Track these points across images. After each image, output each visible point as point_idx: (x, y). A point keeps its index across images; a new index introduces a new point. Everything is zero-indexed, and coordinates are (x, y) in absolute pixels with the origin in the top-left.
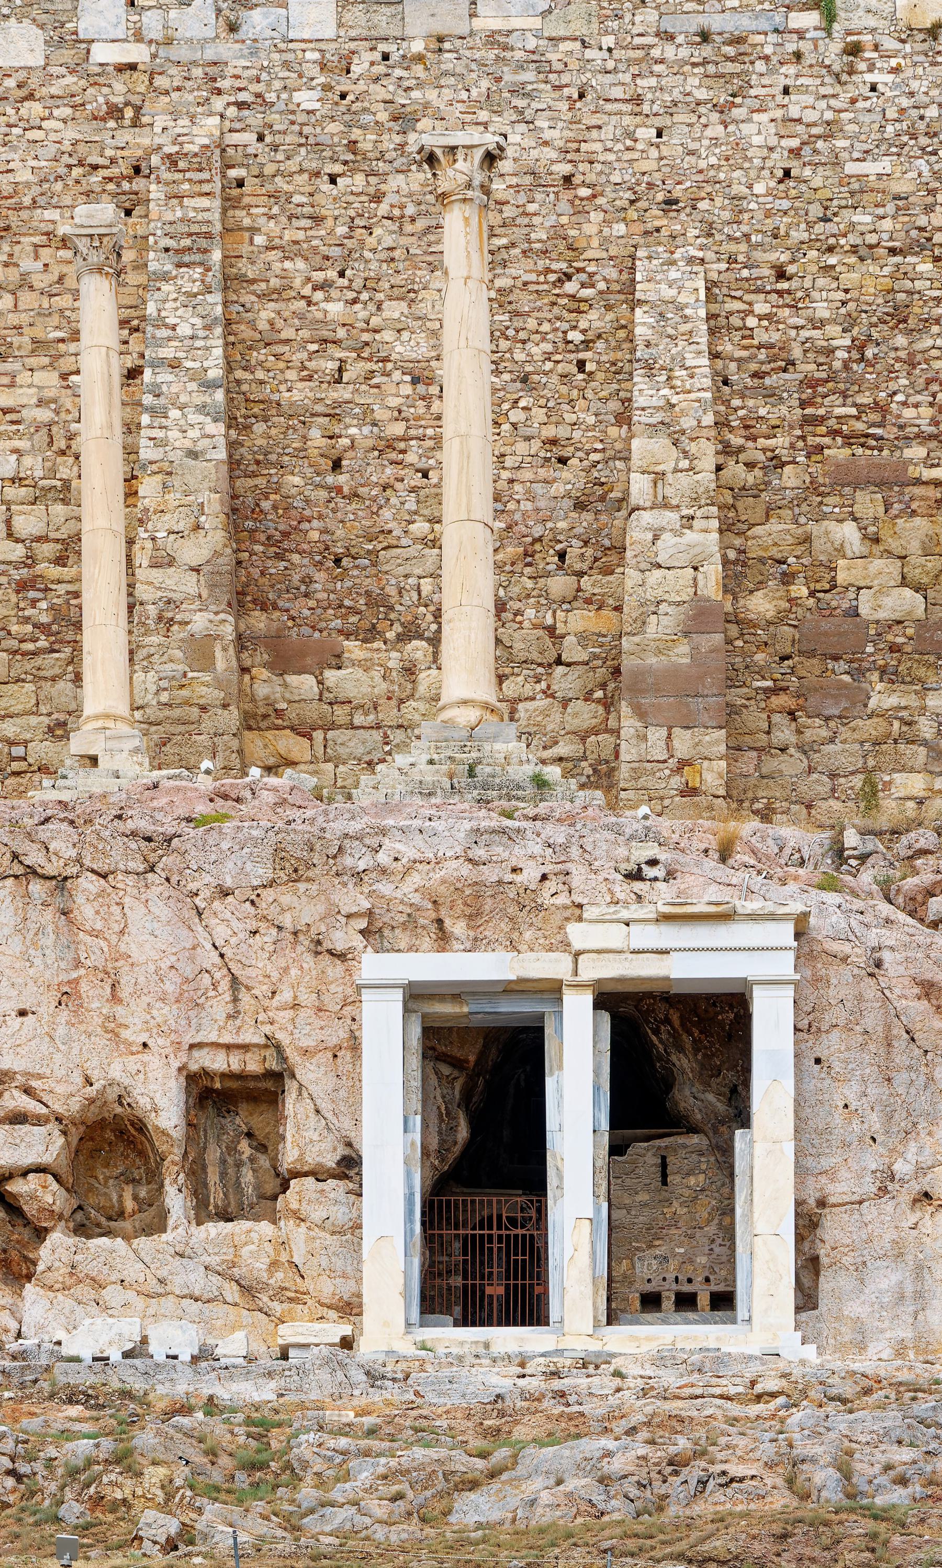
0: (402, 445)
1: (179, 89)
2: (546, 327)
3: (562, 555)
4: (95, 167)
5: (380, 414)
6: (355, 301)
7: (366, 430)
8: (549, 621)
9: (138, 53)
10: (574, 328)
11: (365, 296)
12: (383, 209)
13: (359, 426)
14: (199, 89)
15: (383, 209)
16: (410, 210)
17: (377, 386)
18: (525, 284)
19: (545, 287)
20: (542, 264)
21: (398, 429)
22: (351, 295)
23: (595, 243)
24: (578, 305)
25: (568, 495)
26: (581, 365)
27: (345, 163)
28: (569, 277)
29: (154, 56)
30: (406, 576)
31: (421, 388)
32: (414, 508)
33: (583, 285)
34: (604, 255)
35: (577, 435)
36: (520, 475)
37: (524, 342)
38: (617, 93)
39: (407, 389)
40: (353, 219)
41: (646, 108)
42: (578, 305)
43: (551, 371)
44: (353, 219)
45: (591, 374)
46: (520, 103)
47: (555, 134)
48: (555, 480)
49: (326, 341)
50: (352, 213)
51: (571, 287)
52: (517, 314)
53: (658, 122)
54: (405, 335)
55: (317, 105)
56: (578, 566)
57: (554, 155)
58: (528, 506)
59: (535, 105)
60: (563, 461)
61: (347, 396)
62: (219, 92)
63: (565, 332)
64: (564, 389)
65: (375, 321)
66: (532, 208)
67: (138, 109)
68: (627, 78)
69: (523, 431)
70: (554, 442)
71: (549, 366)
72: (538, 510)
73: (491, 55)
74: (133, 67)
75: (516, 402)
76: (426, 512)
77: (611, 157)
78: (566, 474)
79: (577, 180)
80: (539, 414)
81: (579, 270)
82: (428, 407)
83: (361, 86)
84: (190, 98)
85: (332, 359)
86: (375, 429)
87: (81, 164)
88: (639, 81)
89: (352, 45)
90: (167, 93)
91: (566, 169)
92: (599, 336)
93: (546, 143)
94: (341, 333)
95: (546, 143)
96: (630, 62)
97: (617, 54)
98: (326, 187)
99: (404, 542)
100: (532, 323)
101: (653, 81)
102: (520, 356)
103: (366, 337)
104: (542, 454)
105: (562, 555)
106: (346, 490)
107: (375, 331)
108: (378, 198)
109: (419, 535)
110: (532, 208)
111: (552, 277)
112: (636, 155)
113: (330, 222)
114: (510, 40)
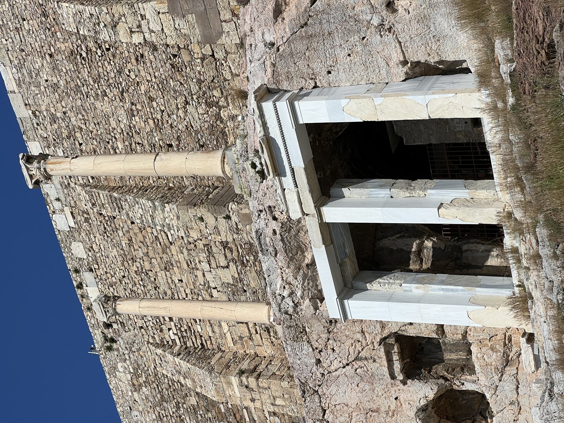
0: (156, 120)
1: (73, 198)
2: (100, 64)
3: (175, 56)
4: (105, 228)
5: (148, 129)
6: (115, 138)
7: (155, 135)
8: (199, 61)
9: (67, 210)
10: (97, 53)
11: (112, 134)
12: (83, 127)
13: (155, 137)
14: (70, 191)
15: (83, 127)
16: (80, 116)
17: (140, 130)
18: (89, 73)
19: (87, 64)
20: (81, 66)
21: (151, 122)
22: (114, 140)
23: (67, 45)
24: (88, 50)
25: (153, 54)
26: (108, 50)
27: (74, 140)
28: (81, 55)
29: (66, 206)
30: (200, 119)
31: (135, 113)
32: (175, 116)
33: (82, 50)
34: (69, 40)
35: (131, 50)
36: (152, 74)
37: (108, 73)
38: (17, 36)
39: (137, 118)
40: (90, 138)
41: (18, 26)
42: (88, 50)
43: (113, 62)
44: (90, 138)
45: (109, 46)
46: (34, 75)
47: (38, 61)
48: (149, 59)
49: (131, 149)
50: (88, 138)
51: (84, 55)
52: (99, 76)
53: (21, 21)
54: (120, 119)
55: (61, 150)
56: (177, 50)
57: (45, 62)
58: (161, 70)
59: (33, 69)
60: (142, 56)
61: (146, 142)
62: (69, 184)
63: (99, 56)
64: (118, 56)
65: (119, 131)
66: (64, 70)
67: (83, 212)
68: (12, 33)
69: (137, 73)
70: (137, 60)
71: (112, 63)
72: (162, 66)
73: (23, 86)
74: (72, 213)
75: (128, 76)
76: (176, 111)
77: (38, 39)
78: (146, 54)
79: (49, 52)
80: (129, 66)
81: (78, 51)
82: (140, 110)
83: (49, 133)
84: (74, 194)
85: (136, 147)
86: (154, 131)
87: (105, 233)
88: (12, 29)
89: (39, 137)
90: (75, 202)
91: (47, 57)
92: (96, 42)
93: (43, 65)
94: (127, 143)
95: (43, 65)
96: (7, 33)
97: (7, 38)
98: (83, 147)
99: (188, 120)
100: (101, 70)
101: (10, 23)
102: (112, 75)
103: (125, 134)
104: (142, 64)
105: (175, 56)
106: (177, 143)
107: (122, 130)
108: (81, 129)
109: (184, 114)
110: (64, 70)
111: (83, 62)
112: (34, 29)
113: (94, 146)
114: (17, 78)
